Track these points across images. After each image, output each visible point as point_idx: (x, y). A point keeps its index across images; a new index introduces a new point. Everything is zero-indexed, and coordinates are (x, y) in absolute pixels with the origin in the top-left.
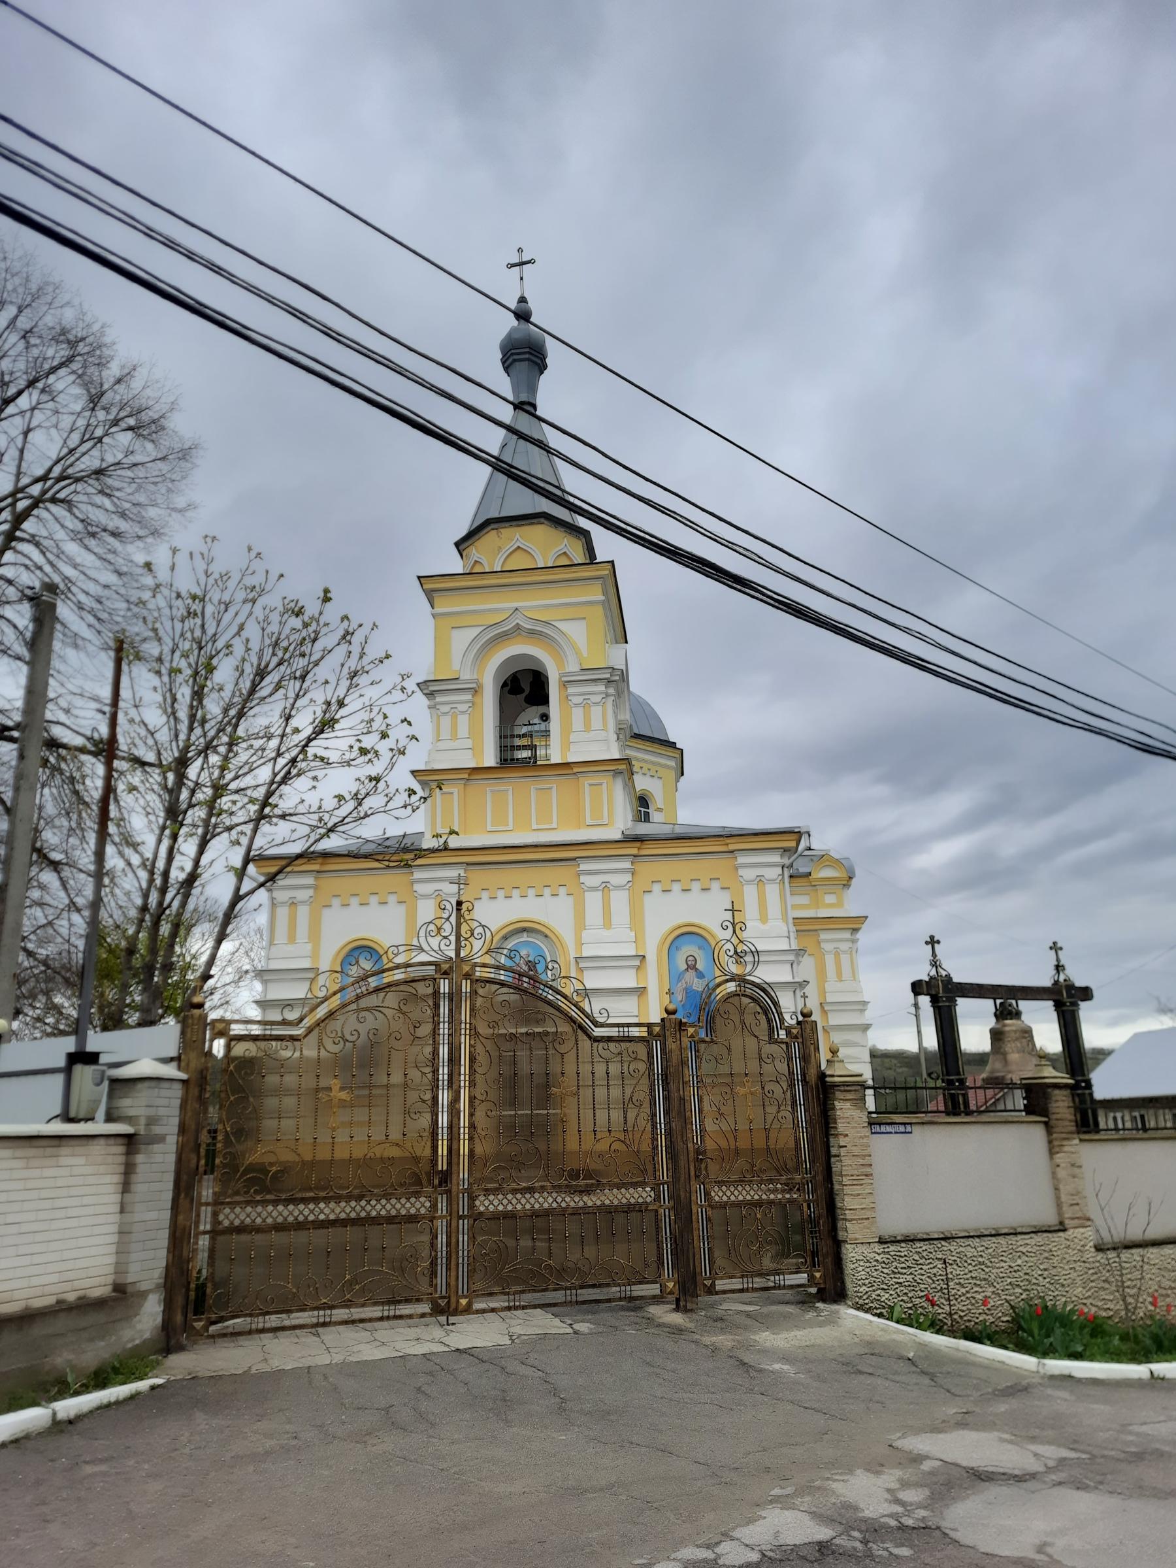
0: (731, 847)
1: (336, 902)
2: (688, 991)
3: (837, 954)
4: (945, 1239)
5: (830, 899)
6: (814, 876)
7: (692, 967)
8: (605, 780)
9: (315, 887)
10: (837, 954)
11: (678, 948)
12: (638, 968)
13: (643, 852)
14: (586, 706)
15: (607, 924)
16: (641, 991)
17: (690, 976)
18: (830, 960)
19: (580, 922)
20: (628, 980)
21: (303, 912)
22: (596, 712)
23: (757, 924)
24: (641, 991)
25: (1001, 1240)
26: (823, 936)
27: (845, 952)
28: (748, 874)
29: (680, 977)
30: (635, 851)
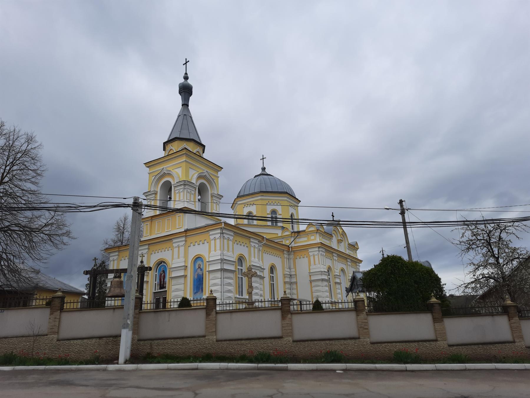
1: (123, 259)
2: (198, 275)
3: (314, 256)
4: (4, 338)
5: (313, 238)
7: (199, 267)
9: (118, 255)
10: (314, 256)
12: (185, 269)
14: (179, 193)
16: (185, 276)
17: (199, 270)
18: (312, 258)
19: (173, 259)
20: (182, 273)
21: (116, 262)
22: (182, 194)
23: (214, 252)
24: (185, 276)
25: (24, 338)
29: (196, 270)
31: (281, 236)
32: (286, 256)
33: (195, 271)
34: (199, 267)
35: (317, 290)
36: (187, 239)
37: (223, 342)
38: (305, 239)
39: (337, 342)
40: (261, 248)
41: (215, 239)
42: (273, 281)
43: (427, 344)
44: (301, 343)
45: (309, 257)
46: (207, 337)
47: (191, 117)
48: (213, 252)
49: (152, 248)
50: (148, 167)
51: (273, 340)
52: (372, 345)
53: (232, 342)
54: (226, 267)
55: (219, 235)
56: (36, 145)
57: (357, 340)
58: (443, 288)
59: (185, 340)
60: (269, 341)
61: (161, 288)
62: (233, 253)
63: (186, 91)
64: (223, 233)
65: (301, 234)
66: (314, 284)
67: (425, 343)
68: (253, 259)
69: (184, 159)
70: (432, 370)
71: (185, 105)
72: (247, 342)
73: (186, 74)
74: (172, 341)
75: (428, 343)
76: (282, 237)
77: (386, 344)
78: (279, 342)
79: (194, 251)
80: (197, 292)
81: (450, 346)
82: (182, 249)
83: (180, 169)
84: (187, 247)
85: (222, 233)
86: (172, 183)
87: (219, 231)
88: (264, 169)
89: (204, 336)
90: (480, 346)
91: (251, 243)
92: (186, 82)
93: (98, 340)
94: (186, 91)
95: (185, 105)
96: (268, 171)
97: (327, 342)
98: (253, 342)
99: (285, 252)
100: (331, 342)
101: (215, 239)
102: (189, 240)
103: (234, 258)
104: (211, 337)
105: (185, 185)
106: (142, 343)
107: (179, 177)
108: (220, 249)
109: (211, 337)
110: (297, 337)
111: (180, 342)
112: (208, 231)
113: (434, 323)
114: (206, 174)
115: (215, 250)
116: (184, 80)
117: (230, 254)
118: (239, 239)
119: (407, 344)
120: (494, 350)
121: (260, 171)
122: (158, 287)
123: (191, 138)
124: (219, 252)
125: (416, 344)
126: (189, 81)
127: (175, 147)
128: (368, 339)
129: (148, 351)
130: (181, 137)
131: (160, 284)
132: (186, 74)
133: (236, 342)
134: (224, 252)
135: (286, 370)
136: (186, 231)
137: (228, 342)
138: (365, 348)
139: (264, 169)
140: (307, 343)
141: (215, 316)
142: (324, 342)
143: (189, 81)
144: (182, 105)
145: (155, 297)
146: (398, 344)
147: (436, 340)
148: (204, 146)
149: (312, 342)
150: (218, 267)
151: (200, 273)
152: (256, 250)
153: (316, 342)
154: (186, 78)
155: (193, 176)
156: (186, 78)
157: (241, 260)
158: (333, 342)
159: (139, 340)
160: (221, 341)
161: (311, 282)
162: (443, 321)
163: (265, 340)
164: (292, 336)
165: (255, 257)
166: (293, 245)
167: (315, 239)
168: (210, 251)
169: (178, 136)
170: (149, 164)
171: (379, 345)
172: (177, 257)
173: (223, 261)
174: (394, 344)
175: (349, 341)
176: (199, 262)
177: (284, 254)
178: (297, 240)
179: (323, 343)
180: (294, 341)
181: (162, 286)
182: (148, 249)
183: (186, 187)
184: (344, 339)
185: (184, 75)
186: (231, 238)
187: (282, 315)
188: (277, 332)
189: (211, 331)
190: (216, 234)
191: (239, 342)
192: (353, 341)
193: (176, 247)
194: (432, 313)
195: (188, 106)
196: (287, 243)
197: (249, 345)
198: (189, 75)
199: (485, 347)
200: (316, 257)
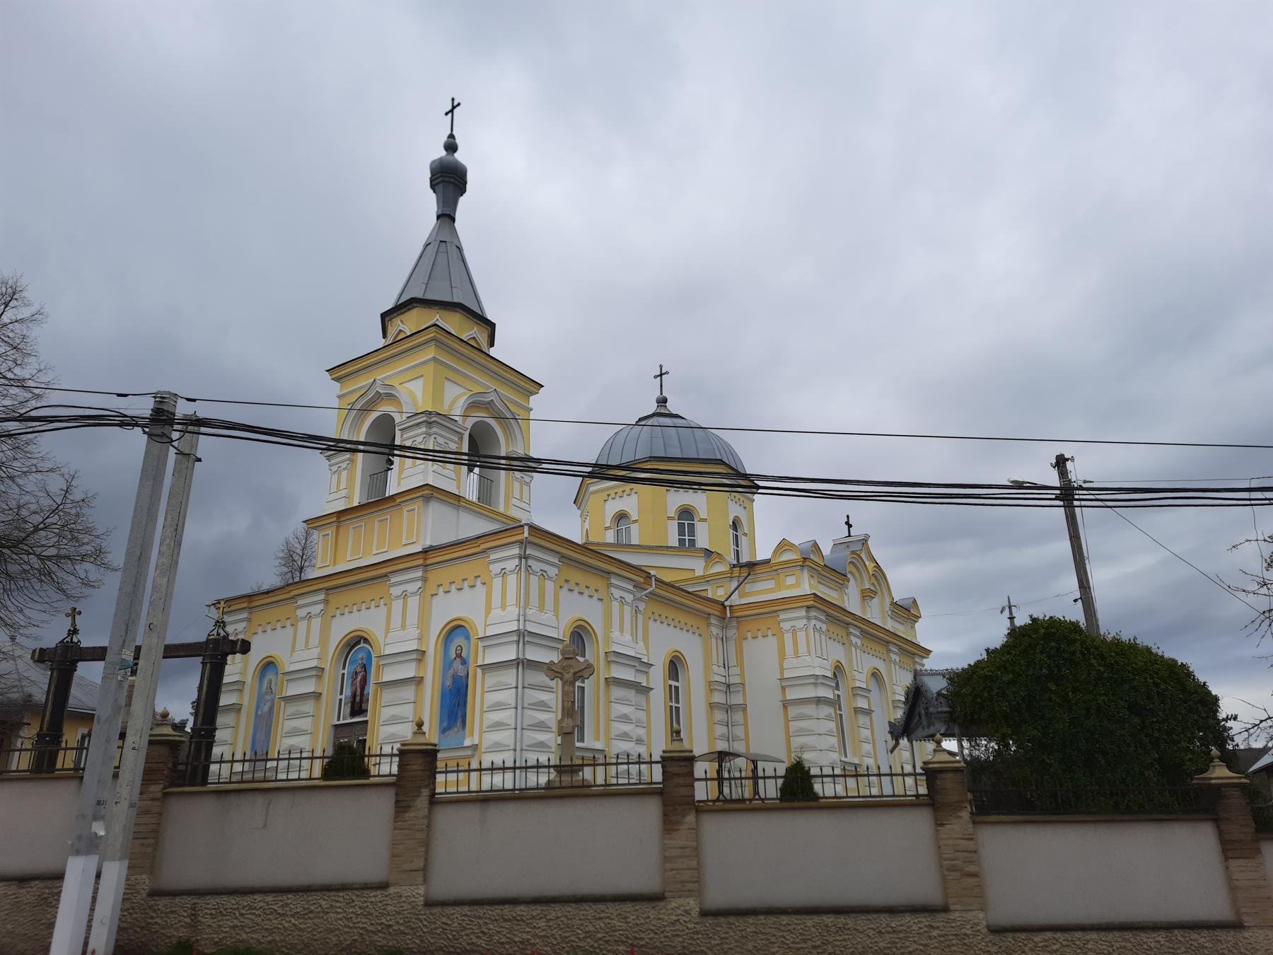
0: (483, 546)
1: (260, 630)
2: (455, 677)
3: (794, 631)
5: (791, 580)
6: (773, 561)
7: (459, 656)
8: (417, 505)
9: (248, 620)
10: (794, 631)
11: (452, 641)
12: (419, 661)
13: (429, 562)
15: (403, 627)
16: (418, 681)
18: (788, 638)
20: (409, 671)
26: (783, 616)
27: (801, 629)
28: (495, 568)
30: (421, 562)
31: (703, 577)
32: (715, 630)
33: (448, 665)
34: (459, 656)
35: (801, 730)
36: (429, 575)
37: (449, 910)
38: (771, 584)
39: (862, 922)
40: (642, 606)
41: (503, 573)
42: (677, 701)
44: (732, 919)
45: (779, 634)
46: (392, 890)
47: (459, 249)
48: (496, 613)
49: (337, 599)
50: (337, 380)
51: (628, 907)
52: (996, 938)
53: (481, 911)
54: (533, 654)
55: (516, 561)
56: (25, 313)
57: (940, 917)
58: (1226, 729)
59: (313, 897)
60: (613, 909)
61: (354, 713)
62: (557, 616)
63: (449, 179)
64: (526, 558)
65: (759, 569)
66: (793, 711)
67: (1194, 936)
68: (616, 634)
69: (430, 352)
71: (447, 217)
72: (536, 910)
73: (451, 136)
74: (269, 898)
75: (1205, 933)
76: (706, 579)
77: (1049, 935)
78: (652, 914)
79: (446, 609)
80: (449, 728)
82: (414, 602)
83: (421, 381)
84: (426, 597)
85: (524, 557)
86: (398, 418)
87: (515, 551)
88: (662, 401)
89: (383, 886)
91: (613, 590)
92: (450, 157)
93: (13, 889)
94: (449, 179)
95: (447, 217)
96: (672, 407)
97: (828, 919)
98: (554, 911)
99: (713, 621)
100: (842, 920)
101: (503, 573)
102: (436, 576)
103: (560, 629)
104: (406, 891)
105: (429, 424)
106: (162, 903)
107: (415, 405)
108: (518, 605)
109: (406, 891)
110: (717, 896)
111: (296, 903)
112: (484, 551)
113: (1226, 859)
114: (492, 397)
115: (503, 607)
116: (444, 153)
117: (547, 617)
118: (576, 576)
119: (1128, 935)
121: (652, 408)
122: (346, 710)
123: (456, 300)
124: (513, 611)
125: (1161, 937)
126: (459, 156)
127: (410, 323)
128: (981, 915)
129: (183, 933)
130: (428, 297)
131: (353, 703)
132: (451, 136)
133: (496, 911)
134: (530, 612)
136: (426, 552)
137: (466, 909)
138: (970, 947)
139: (662, 401)
140: (751, 920)
141: (425, 812)
142: (816, 919)
143: (459, 156)
144: (438, 217)
145: (336, 737)
146: (1094, 935)
147: (1237, 926)
148: (491, 326)
149: (772, 919)
150: (510, 653)
151: (462, 673)
152: (627, 609)
153: (785, 919)
154: (451, 147)
155: (455, 400)
156: (451, 147)
157: (580, 635)
158: (849, 921)
159: (155, 893)
160: (443, 904)
161: (786, 704)
162: (1258, 851)
163: (601, 906)
164: (699, 893)
165: (622, 630)
166: (736, 600)
167: (797, 585)
168: (488, 609)
170: (340, 372)
171: (1023, 936)
172: (400, 626)
173: (523, 636)
174: (1078, 934)
175: (908, 919)
176: (459, 641)
177: (709, 625)
178: (748, 587)
179: (810, 921)
180: (705, 913)
181: (356, 708)
182: (326, 601)
183: (434, 430)
184: (891, 910)
185: (445, 139)
186: (552, 571)
187: (665, 815)
188: (644, 878)
189: (407, 867)
190: (506, 559)
191: (507, 910)
192: (924, 920)
193: (398, 597)
194: (1217, 821)
195: (454, 220)
196: (719, 593)
197: (542, 924)
198: (458, 141)
200: (801, 635)
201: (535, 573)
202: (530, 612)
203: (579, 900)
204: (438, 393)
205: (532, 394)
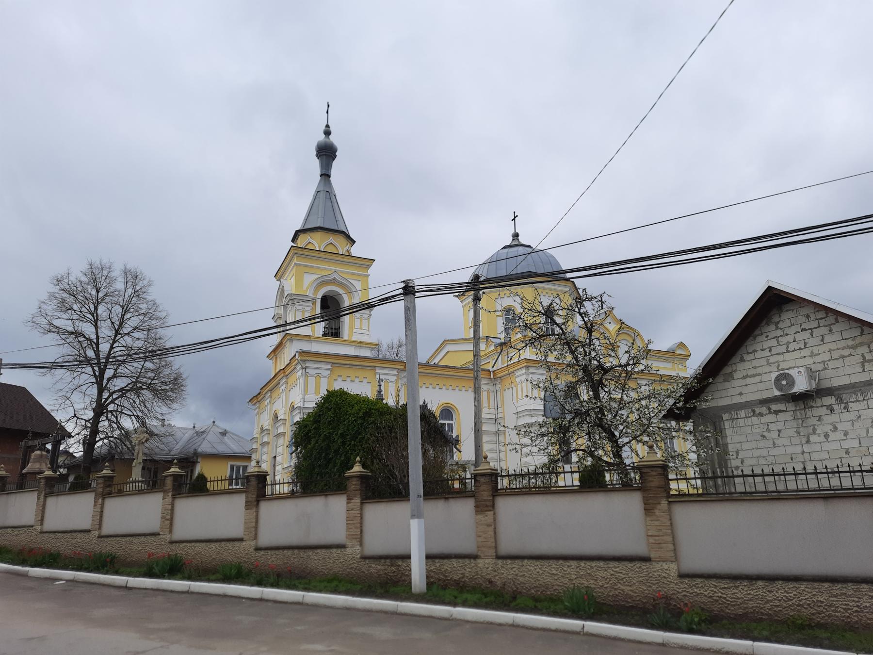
43: (230, 545)
60: (79, 535)
63: (326, 153)
70: (152, 589)
71: (326, 176)
73: (327, 126)
81: (258, 549)
88: (516, 236)
90: (296, 551)
92: (327, 140)
94: (326, 153)
95: (326, 176)
96: (522, 240)
97: (128, 539)
110: (105, 531)
120: (315, 560)
121: (509, 241)
125: (217, 545)
126: (332, 138)
130: (306, 227)
132: (327, 126)
135: (25, 575)
139: (516, 236)
146: (198, 544)
153: (118, 539)
154: (327, 133)
156: (327, 133)
169: (322, 226)
175: (149, 537)
184: (145, 535)
192: (153, 538)
198: (331, 129)
199: (302, 553)
201: (312, 376)
202: (307, 397)
203: (71, 532)
204: (299, 282)
205: (369, 266)
